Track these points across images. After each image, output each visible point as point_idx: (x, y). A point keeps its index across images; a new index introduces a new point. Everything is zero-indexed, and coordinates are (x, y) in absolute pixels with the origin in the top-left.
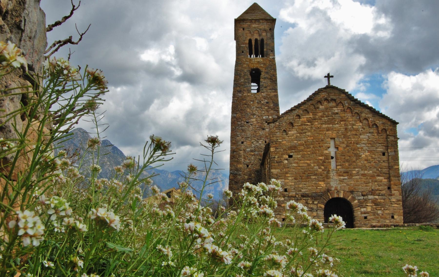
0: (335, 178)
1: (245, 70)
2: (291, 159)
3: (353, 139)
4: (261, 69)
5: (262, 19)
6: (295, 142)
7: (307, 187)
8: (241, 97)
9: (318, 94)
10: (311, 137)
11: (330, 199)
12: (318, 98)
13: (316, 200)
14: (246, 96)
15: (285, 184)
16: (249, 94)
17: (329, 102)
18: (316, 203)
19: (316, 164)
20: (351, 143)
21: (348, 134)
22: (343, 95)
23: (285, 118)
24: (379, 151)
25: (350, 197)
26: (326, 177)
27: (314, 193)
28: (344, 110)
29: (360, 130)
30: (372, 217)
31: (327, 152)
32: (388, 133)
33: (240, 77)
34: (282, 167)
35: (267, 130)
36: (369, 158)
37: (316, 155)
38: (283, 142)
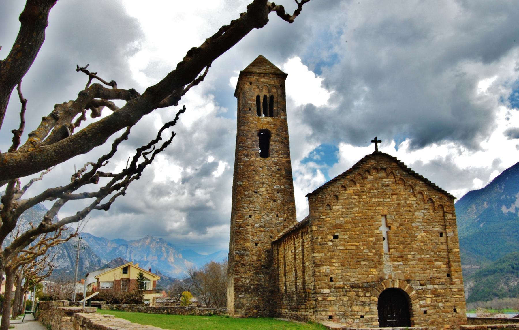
0: (389, 263)
1: (253, 131)
2: (337, 240)
3: (406, 217)
4: (271, 130)
5: (272, 74)
6: (341, 219)
7: (356, 276)
8: (248, 161)
9: (365, 161)
11: (385, 290)
13: (368, 291)
14: (253, 161)
15: (331, 272)
16: (257, 159)
17: (378, 172)
18: (368, 295)
19: (365, 247)
20: (405, 221)
21: (401, 211)
22: (394, 164)
23: (329, 189)
24: (435, 231)
25: (407, 287)
26: (378, 263)
27: (365, 282)
28: (396, 181)
29: (414, 206)
30: (433, 311)
31: (378, 232)
32: (445, 210)
33: (247, 138)
34: (326, 250)
35: (279, 201)
36: (426, 239)
37: (366, 236)
38: (327, 219)
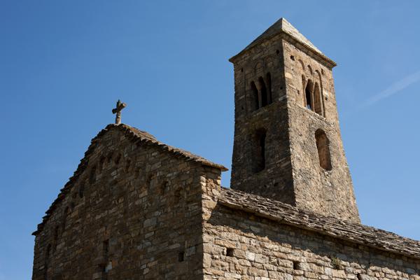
10: (80, 247)
12: (94, 158)
23: (53, 219)
33: (239, 152)
